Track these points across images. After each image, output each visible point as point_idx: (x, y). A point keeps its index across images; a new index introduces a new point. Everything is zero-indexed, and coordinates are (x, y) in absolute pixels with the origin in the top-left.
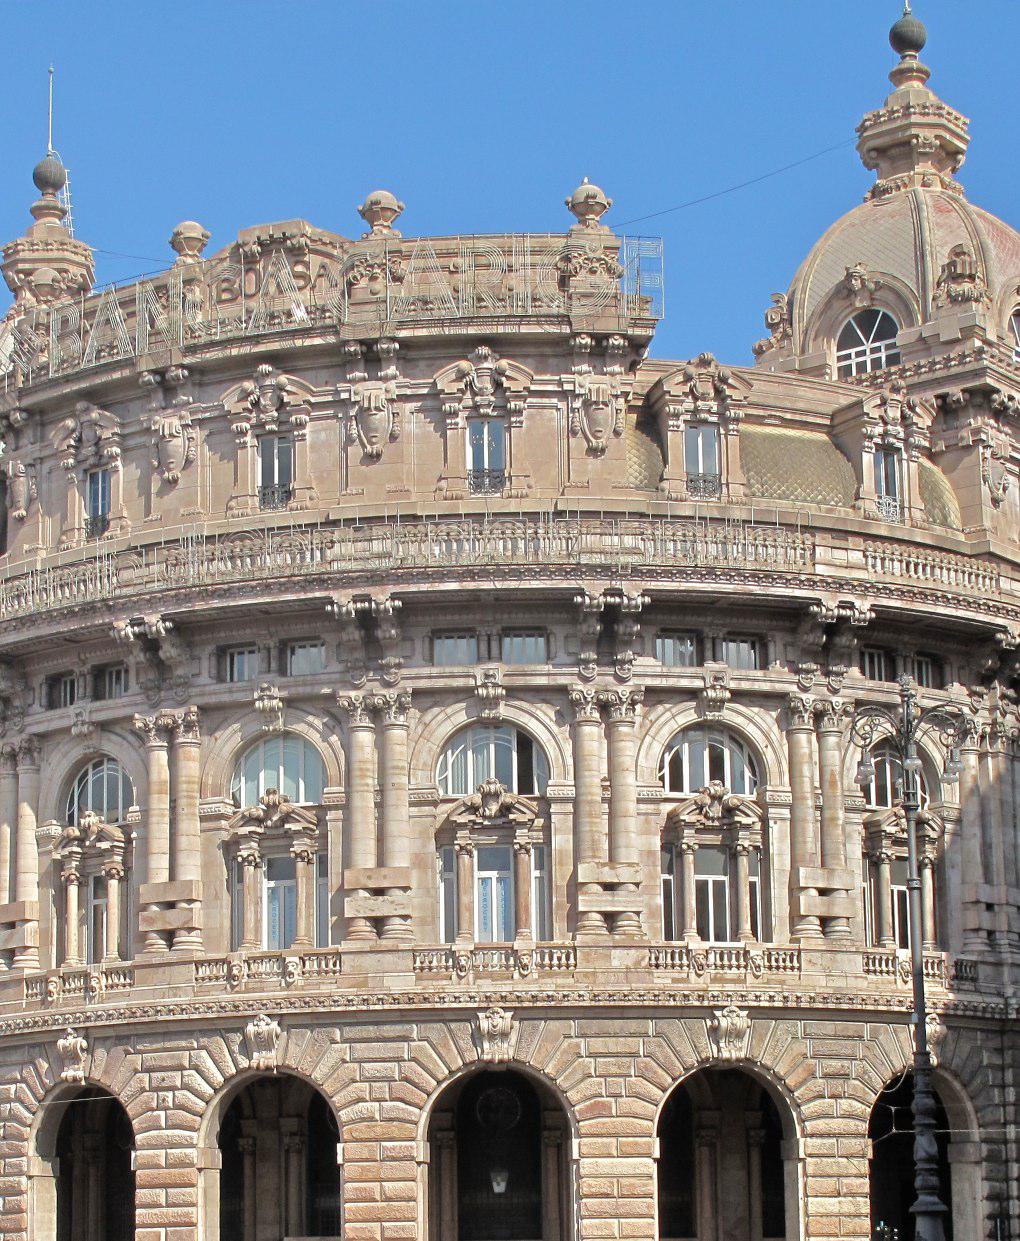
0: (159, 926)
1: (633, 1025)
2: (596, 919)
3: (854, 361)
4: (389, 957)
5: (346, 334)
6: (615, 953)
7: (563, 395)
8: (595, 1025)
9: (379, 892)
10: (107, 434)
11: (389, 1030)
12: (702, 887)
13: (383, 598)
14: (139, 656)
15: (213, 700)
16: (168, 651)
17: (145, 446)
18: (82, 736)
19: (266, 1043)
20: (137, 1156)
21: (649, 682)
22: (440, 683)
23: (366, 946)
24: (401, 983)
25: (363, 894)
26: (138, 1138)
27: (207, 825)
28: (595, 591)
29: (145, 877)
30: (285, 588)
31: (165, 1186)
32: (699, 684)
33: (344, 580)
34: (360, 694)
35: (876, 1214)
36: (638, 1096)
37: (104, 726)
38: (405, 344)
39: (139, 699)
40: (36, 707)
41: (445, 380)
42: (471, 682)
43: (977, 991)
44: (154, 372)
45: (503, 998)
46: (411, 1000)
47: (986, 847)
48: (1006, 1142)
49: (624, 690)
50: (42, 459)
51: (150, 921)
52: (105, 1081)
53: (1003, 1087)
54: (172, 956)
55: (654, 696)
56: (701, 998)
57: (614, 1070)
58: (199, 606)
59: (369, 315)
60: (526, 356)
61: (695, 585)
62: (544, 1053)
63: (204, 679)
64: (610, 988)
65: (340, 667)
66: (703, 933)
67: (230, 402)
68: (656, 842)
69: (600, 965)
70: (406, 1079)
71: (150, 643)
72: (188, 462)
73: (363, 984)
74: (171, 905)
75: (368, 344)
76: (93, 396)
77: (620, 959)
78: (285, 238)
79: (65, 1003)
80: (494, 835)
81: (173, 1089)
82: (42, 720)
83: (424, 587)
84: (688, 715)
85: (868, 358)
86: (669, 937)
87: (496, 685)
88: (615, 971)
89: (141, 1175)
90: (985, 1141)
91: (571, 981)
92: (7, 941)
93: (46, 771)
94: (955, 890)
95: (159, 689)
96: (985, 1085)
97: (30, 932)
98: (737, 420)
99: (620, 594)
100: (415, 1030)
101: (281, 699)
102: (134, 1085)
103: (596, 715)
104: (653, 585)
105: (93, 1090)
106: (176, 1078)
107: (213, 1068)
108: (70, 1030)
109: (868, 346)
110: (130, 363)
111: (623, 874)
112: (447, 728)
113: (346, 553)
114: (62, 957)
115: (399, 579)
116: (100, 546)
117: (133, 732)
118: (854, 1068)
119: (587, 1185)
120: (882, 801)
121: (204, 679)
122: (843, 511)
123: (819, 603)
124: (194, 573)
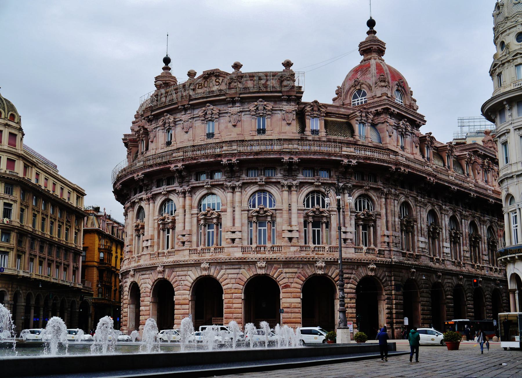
2: (286, 239)
3: (356, 102)
4: (236, 248)
6: (292, 248)
7: (281, 110)
9: (234, 232)
12: (314, 231)
13: (234, 160)
14: (177, 175)
15: (195, 185)
16: (184, 173)
18: (164, 195)
19: (205, 269)
20: (175, 298)
21: (301, 180)
22: (249, 181)
23: (230, 245)
24: (238, 254)
25: (229, 233)
26: (176, 293)
27: (193, 216)
28: (286, 158)
32: (313, 181)
33: (226, 155)
34: (230, 183)
35: (357, 313)
36: (296, 283)
38: (242, 98)
41: (252, 107)
42: (257, 181)
43: (384, 257)
44: (182, 106)
45: (263, 259)
46: (241, 259)
47: (387, 222)
48: (392, 295)
49: (294, 183)
53: (391, 281)
54: (184, 248)
55: (302, 184)
56: (313, 259)
57: (291, 276)
59: (233, 91)
60: (271, 101)
61: (312, 157)
62: (273, 273)
63: (193, 180)
64: (290, 256)
65: (225, 177)
66: (314, 243)
68: (302, 220)
69: (287, 250)
70: (239, 278)
73: (229, 255)
74: (184, 235)
75: (233, 98)
76: (168, 112)
77: (293, 249)
78: (214, 73)
82: (156, 190)
83: (245, 157)
84: (311, 189)
85: (360, 101)
86: (306, 243)
87: (263, 182)
88: (291, 252)
89: (176, 302)
90: (386, 294)
91: (280, 254)
93: (156, 202)
94: (379, 233)
95: (182, 183)
96: (386, 280)
98: (323, 116)
99: (293, 159)
100: (243, 267)
101: (210, 185)
103: (287, 189)
104: (301, 157)
106: (183, 278)
107: (193, 275)
109: (360, 99)
110: (176, 103)
111: (294, 228)
112: (251, 192)
114: (159, 248)
115: (239, 156)
116: (170, 148)
117: (176, 193)
118: (352, 276)
120: (360, 210)
121: (193, 180)
122: (351, 139)
123: (343, 161)
124: (190, 154)
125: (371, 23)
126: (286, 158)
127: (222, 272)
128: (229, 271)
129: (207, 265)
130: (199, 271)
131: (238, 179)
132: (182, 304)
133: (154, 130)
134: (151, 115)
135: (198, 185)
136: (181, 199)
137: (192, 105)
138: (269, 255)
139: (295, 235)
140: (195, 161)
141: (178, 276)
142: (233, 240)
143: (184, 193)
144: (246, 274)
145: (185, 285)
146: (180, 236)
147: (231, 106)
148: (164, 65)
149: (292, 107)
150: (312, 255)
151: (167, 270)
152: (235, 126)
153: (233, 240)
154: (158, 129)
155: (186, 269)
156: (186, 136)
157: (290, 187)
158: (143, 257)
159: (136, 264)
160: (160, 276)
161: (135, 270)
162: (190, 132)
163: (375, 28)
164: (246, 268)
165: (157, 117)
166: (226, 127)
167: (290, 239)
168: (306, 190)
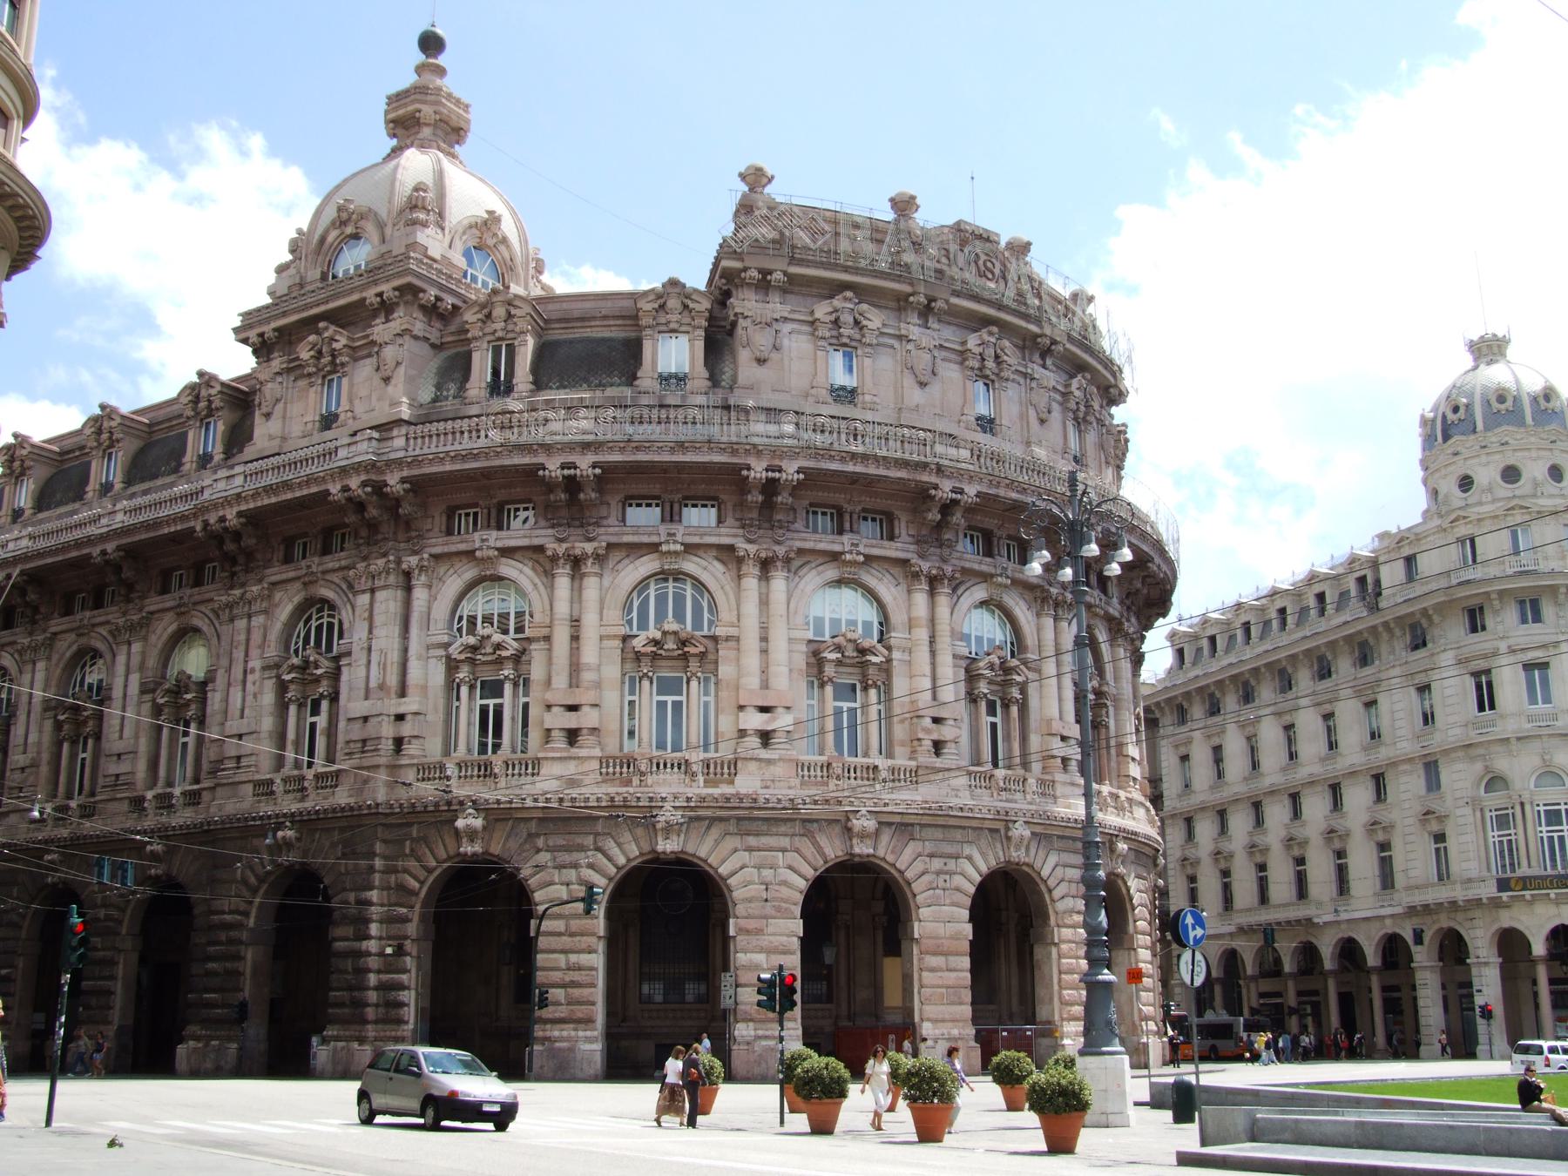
0: (935, 736)
5: (1048, 331)
10: (871, 325)
17: (892, 347)
18: (854, 563)
37: (869, 559)
39: (912, 547)
40: (799, 525)
50: (786, 319)
51: (928, 731)
52: (890, 858)
58: (1002, 492)
74: (936, 720)
81: (951, 873)
92: (768, 722)
102: (919, 866)
106: (952, 864)
108: (864, 810)
127: (1053, 859)
130: (999, 845)
132: (945, 954)
133: (776, 326)
134: (785, 273)
135: (976, 567)
136: (921, 599)
140: (1014, 495)
141: (931, 856)
143: (934, 582)
145: (958, 889)
146: (928, 721)
147: (1037, 357)
148: (420, 57)
152: (1042, 421)
154: (786, 328)
155: (958, 835)
156: (915, 396)
158: (753, 766)
159: (699, 789)
160: (862, 849)
162: (935, 389)
165: (793, 286)
166: (1023, 417)
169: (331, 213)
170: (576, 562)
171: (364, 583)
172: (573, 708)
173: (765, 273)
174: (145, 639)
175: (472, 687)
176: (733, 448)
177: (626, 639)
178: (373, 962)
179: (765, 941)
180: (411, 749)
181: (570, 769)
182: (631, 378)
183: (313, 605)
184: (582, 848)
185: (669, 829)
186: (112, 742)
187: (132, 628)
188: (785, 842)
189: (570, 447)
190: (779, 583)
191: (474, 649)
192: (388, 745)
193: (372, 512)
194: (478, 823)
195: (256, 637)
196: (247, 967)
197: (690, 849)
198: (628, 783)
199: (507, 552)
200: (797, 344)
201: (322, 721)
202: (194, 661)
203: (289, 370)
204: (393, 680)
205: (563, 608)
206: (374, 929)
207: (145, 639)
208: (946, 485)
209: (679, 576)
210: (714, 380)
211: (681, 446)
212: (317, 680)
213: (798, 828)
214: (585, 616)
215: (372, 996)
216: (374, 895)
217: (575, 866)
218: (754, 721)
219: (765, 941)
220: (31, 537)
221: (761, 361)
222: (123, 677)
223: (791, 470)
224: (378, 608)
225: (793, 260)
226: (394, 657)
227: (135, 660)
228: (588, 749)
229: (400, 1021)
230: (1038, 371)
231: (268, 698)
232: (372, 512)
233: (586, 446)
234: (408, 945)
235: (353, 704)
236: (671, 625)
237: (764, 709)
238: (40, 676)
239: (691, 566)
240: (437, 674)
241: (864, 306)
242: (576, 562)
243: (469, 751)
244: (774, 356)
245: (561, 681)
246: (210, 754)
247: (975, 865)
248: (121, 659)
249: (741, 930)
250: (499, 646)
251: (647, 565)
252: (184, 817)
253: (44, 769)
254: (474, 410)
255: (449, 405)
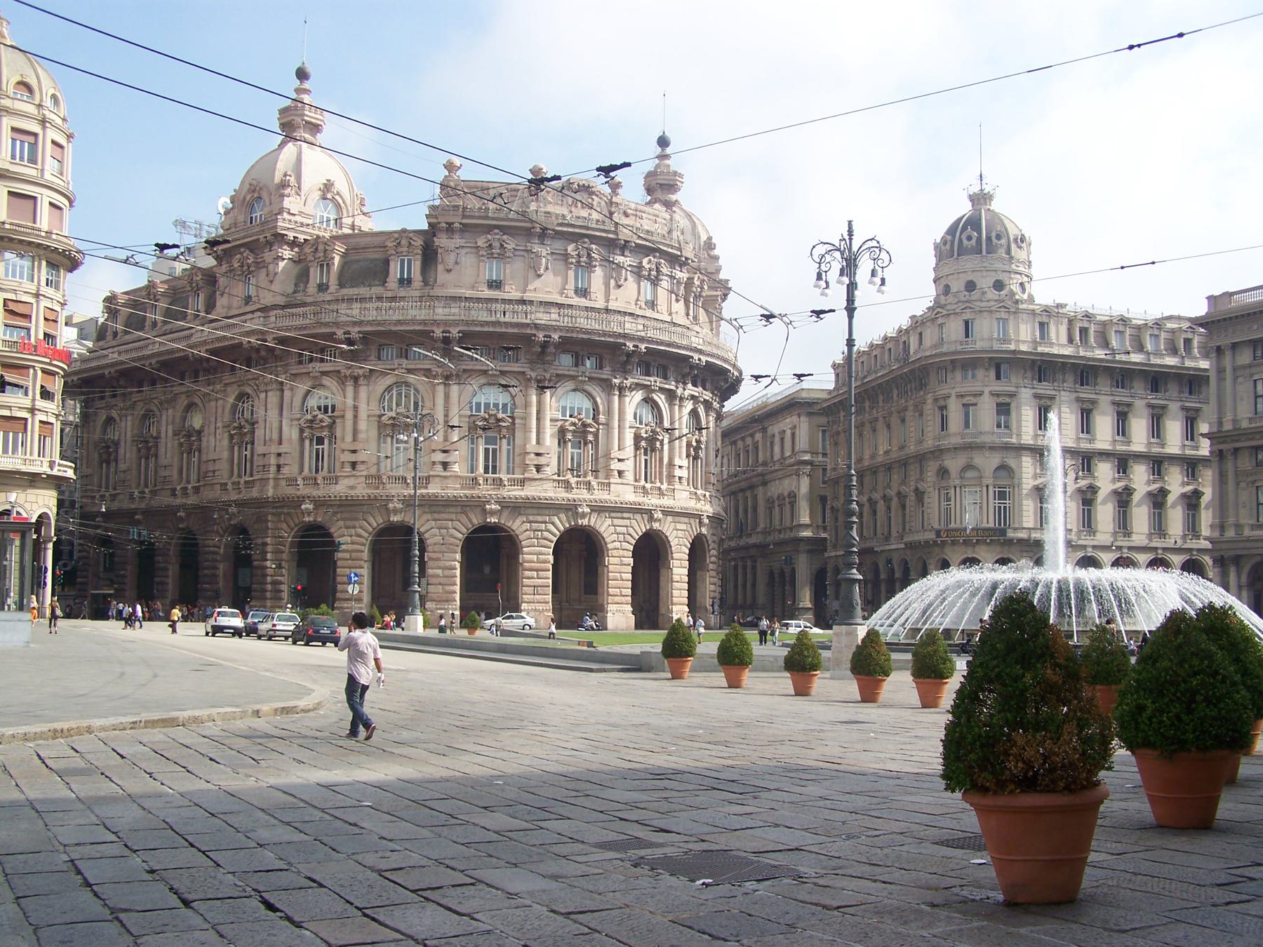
1: (686, 520)
8: (677, 519)
11: (625, 515)
16: (551, 349)
29: (526, 440)
30: (610, 336)
31: (537, 570)
49: (687, 393)
54: (539, 476)
58: (575, 335)
67: (571, 248)
71: (545, 345)
72: (547, 268)
74: (538, 454)
76: (505, 230)
79: (484, 490)
80: (578, 435)
97: (454, 456)
105: (495, 528)
110: (532, 221)
113: (630, 327)
115: (649, 342)
119: (676, 578)
125: (663, 142)
126: (696, 356)
128: (616, 522)
129: (587, 510)
131: (625, 373)
137: (557, 232)
138: (666, 502)
139: (684, 473)
142: (620, 473)
144: (639, 527)
149: (682, 275)
150: (699, 506)
151: (506, 513)
153: (620, 473)
154: (464, 251)
155: (547, 512)
157: (681, 399)
158: (437, 479)
161: (403, 501)
163: (668, 151)
164: (638, 517)
165: (465, 228)
166: (607, 286)
167: (680, 478)
168: (689, 406)
169: (247, 186)
170: (356, 379)
171: (262, 388)
172: (354, 452)
173: (450, 224)
174: (174, 407)
175: (311, 440)
176: (424, 322)
177: (380, 416)
178: (269, 571)
179: (441, 564)
180: (285, 470)
181: (351, 482)
182: (384, 282)
183: (242, 397)
184: (357, 519)
185: (395, 511)
186: (163, 461)
187: (168, 402)
188: (453, 516)
189: (346, 324)
190: (455, 389)
191: (311, 421)
192: (273, 469)
193: (263, 353)
194: (311, 507)
195: (220, 410)
196: (221, 572)
197: (407, 519)
198: (378, 488)
199: (324, 373)
200: (468, 260)
201: (248, 453)
202: (196, 421)
203: (230, 271)
204: (275, 436)
205: (350, 402)
206: (269, 556)
207: (174, 407)
208: (541, 336)
209: (407, 385)
210: (425, 282)
211: (399, 322)
212: (245, 434)
213: (459, 510)
214: (362, 405)
215: (269, 587)
216: (269, 540)
217: (354, 527)
218: (439, 457)
219: (441, 564)
220: (120, 353)
221: (449, 271)
222: (166, 427)
223: (454, 332)
224: (269, 400)
225: (464, 217)
226: (276, 425)
227: (170, 419)
228: (362, 471)
229: (281, 599)
230: (619, 259)
231: (226, 442)
232: (263, 353)
233: (355, 324)
234: (284, 564)
235: (260, 449)
236: (402, 410)
237: (445, 451)
238: (129, 423)
239: (412, 378)
240: (295, 435)
241: (505, 237)
242: (356, 379)
243: (310, 470)
244: (457, 267)
245: (349, 438)
246: (203, 468)
247: (559, 525)
248: (164, 417)
249: (430, 559)
250: (321, 421)
251: (389, 380)
252: (192, 500)
253: (134, 472)
254: (310, 300)
255: (299, 296)
